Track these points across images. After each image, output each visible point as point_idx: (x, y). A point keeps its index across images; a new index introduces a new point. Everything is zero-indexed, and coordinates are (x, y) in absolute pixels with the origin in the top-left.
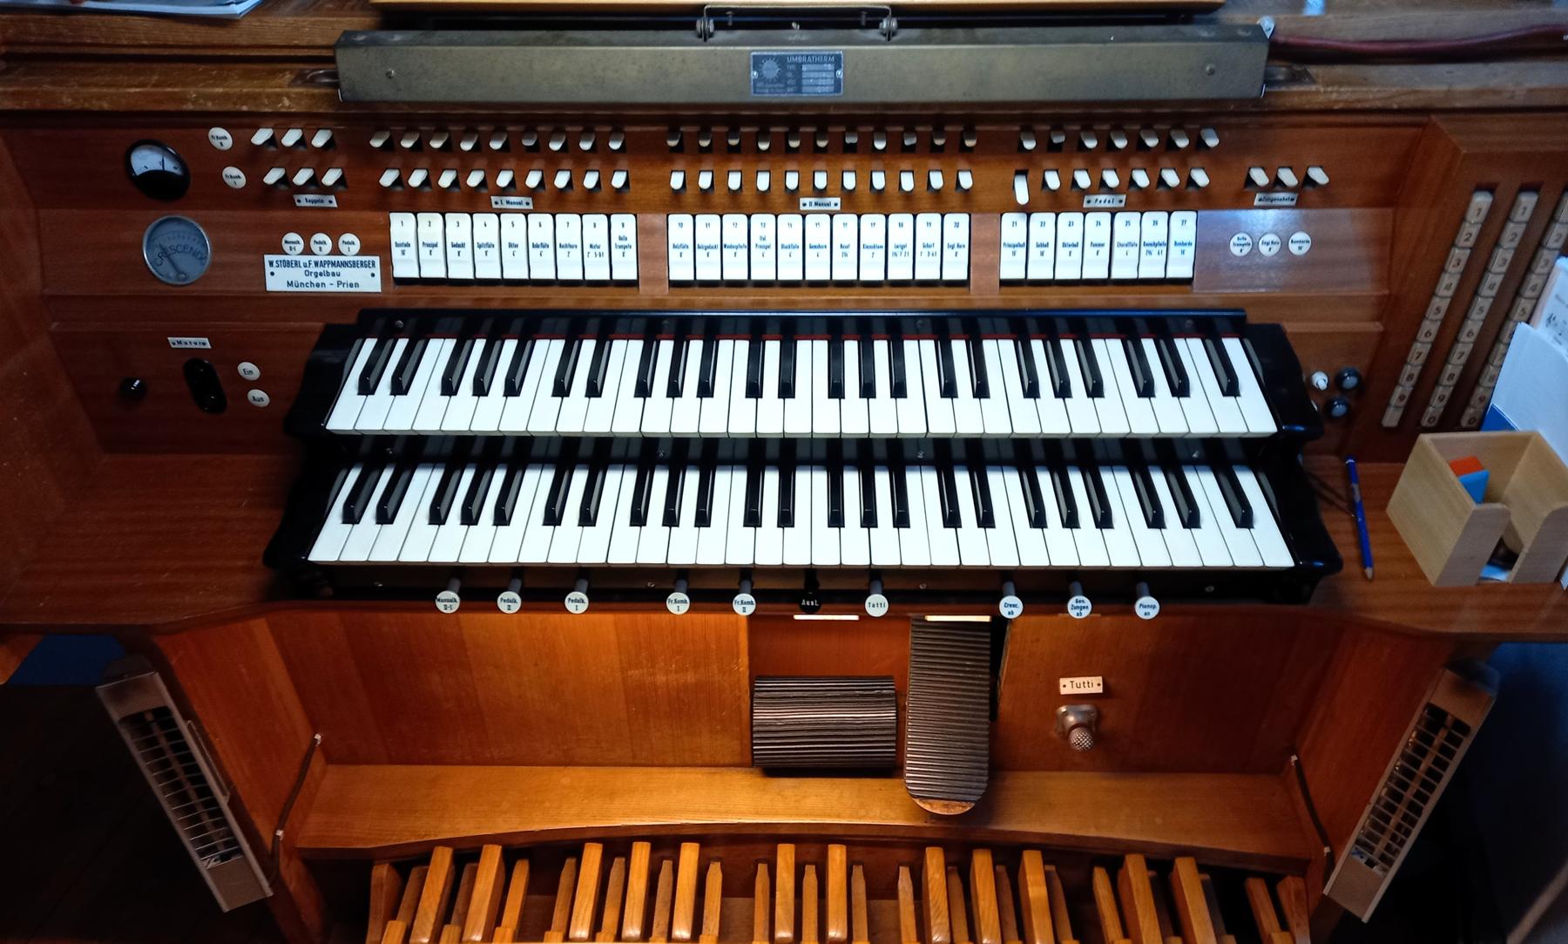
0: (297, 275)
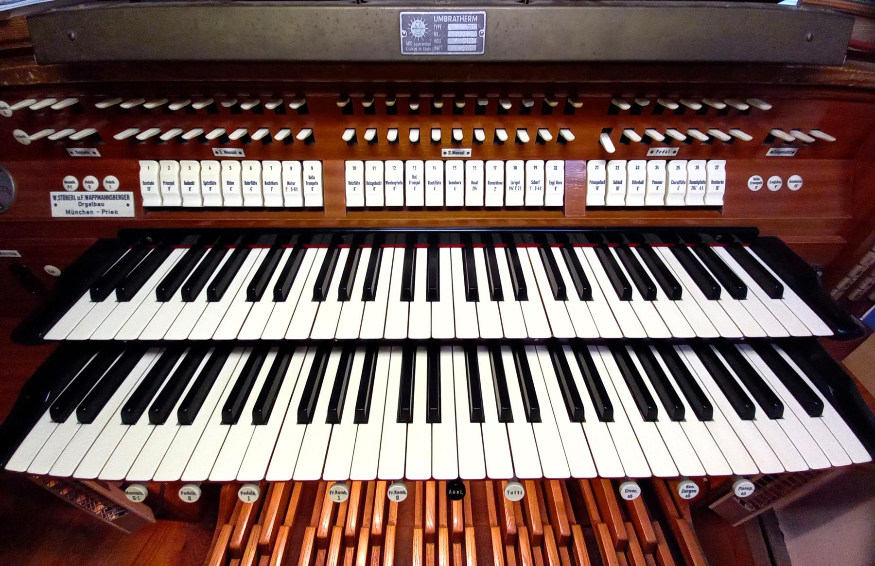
0: (73, 205)
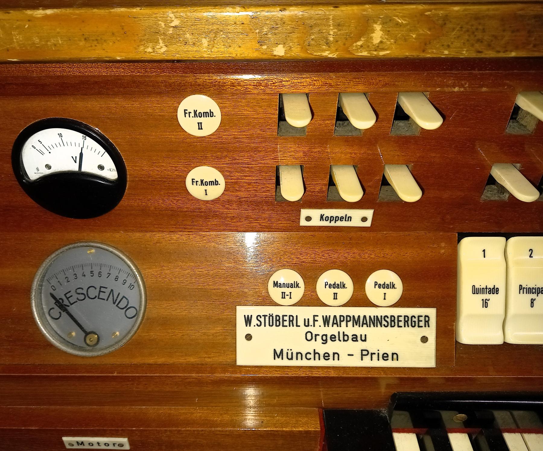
0: (292, 339)
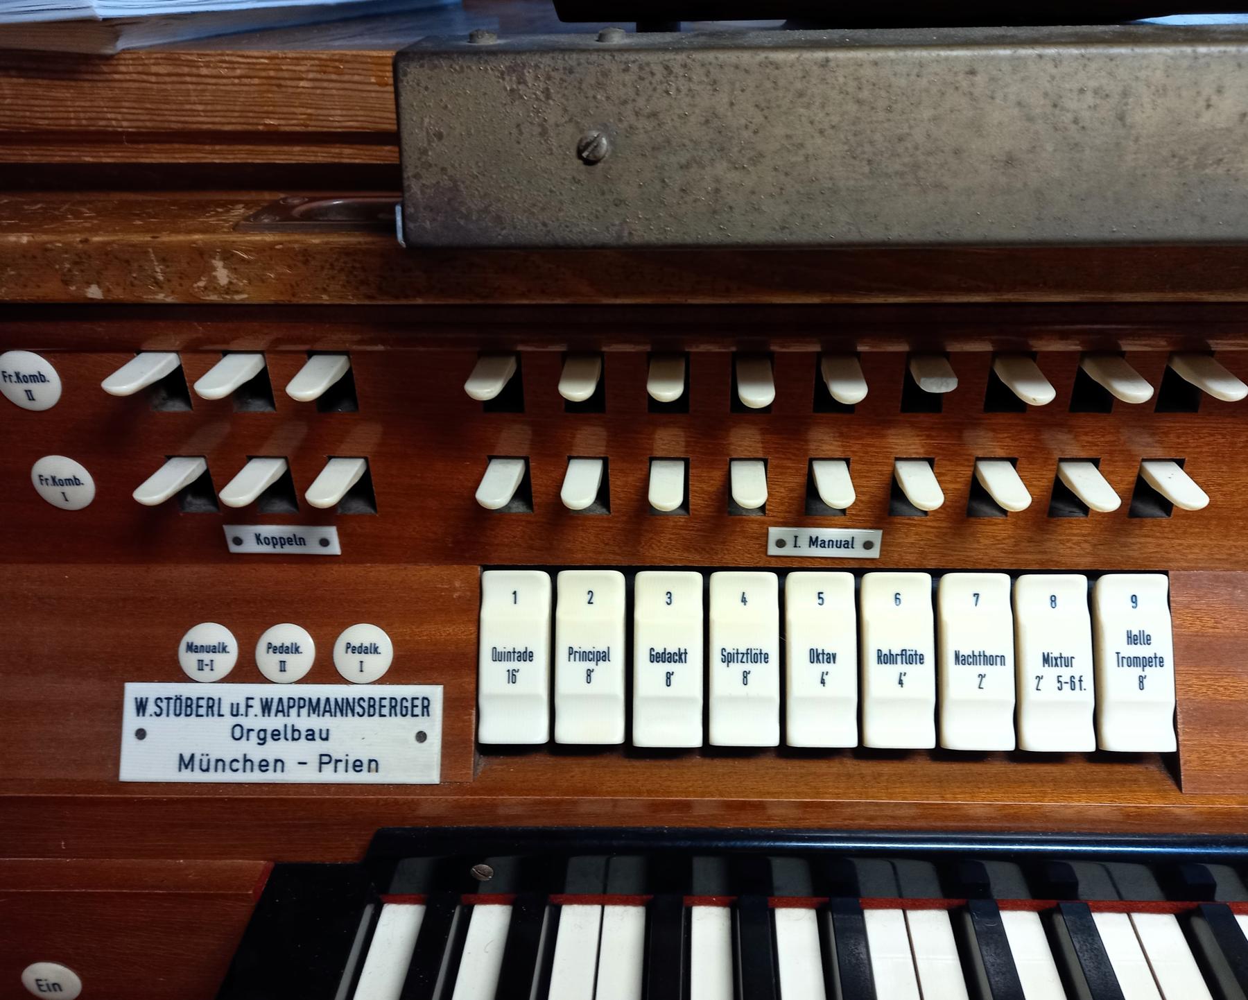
0: (210, 739)
